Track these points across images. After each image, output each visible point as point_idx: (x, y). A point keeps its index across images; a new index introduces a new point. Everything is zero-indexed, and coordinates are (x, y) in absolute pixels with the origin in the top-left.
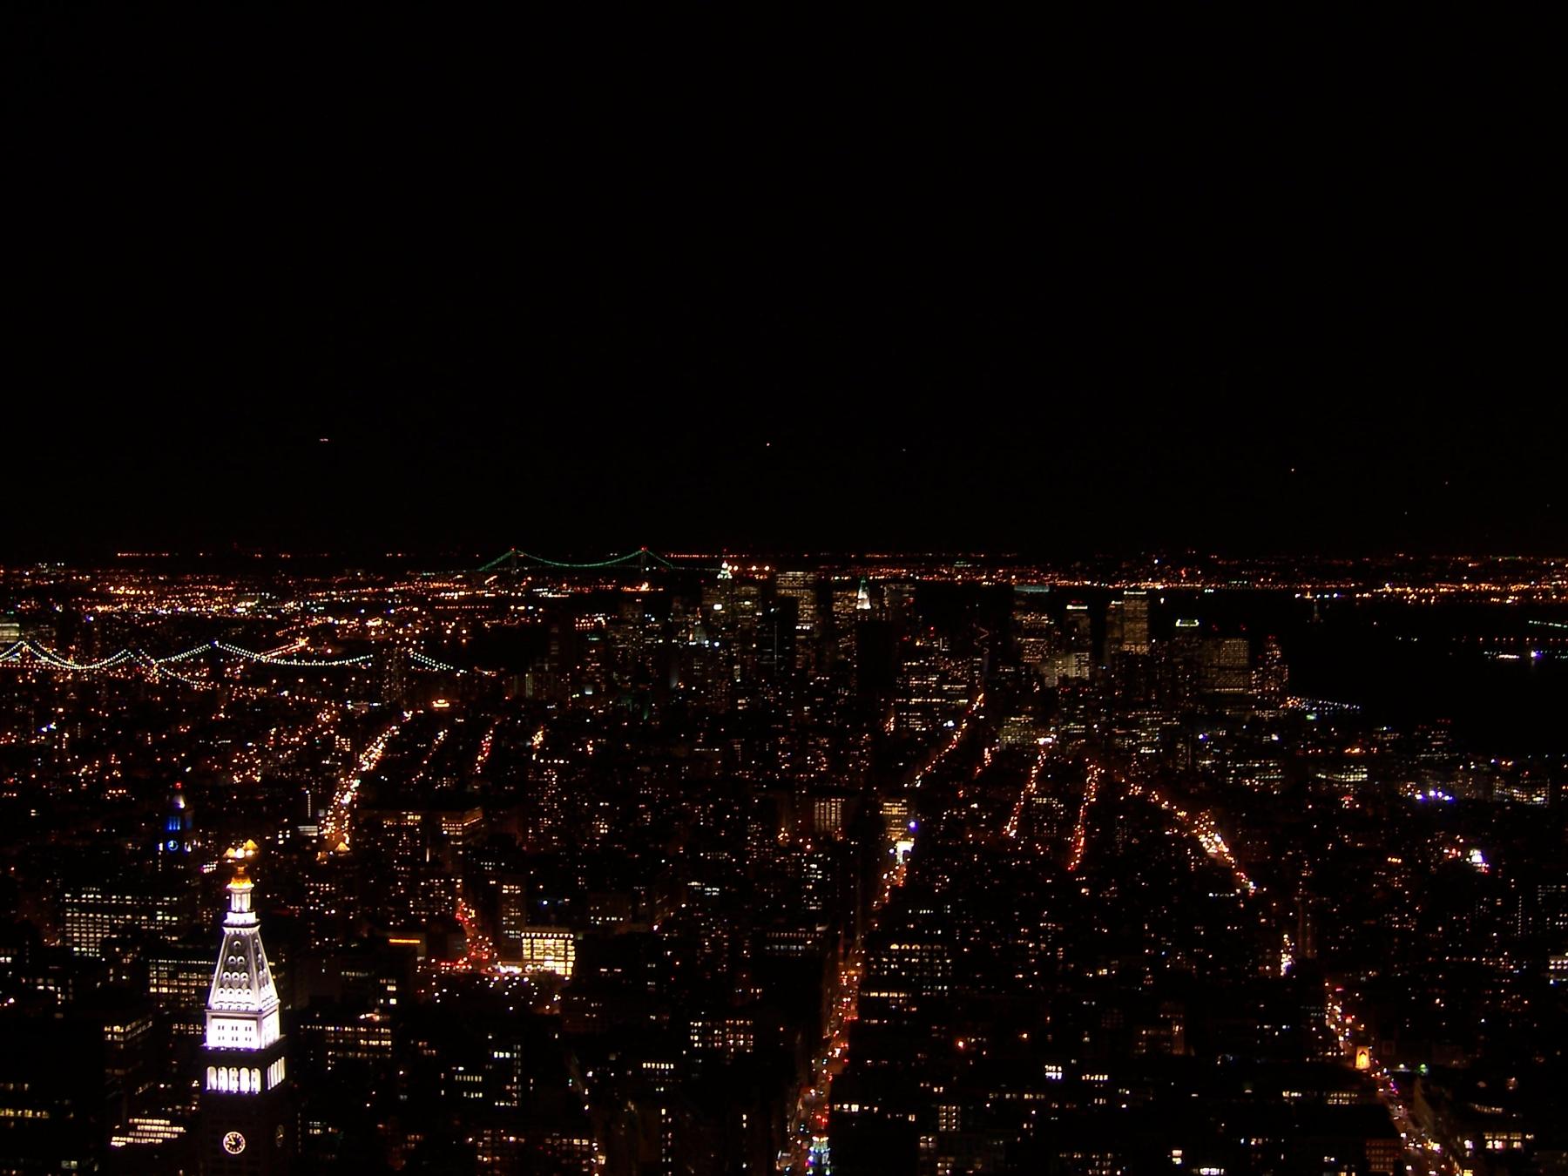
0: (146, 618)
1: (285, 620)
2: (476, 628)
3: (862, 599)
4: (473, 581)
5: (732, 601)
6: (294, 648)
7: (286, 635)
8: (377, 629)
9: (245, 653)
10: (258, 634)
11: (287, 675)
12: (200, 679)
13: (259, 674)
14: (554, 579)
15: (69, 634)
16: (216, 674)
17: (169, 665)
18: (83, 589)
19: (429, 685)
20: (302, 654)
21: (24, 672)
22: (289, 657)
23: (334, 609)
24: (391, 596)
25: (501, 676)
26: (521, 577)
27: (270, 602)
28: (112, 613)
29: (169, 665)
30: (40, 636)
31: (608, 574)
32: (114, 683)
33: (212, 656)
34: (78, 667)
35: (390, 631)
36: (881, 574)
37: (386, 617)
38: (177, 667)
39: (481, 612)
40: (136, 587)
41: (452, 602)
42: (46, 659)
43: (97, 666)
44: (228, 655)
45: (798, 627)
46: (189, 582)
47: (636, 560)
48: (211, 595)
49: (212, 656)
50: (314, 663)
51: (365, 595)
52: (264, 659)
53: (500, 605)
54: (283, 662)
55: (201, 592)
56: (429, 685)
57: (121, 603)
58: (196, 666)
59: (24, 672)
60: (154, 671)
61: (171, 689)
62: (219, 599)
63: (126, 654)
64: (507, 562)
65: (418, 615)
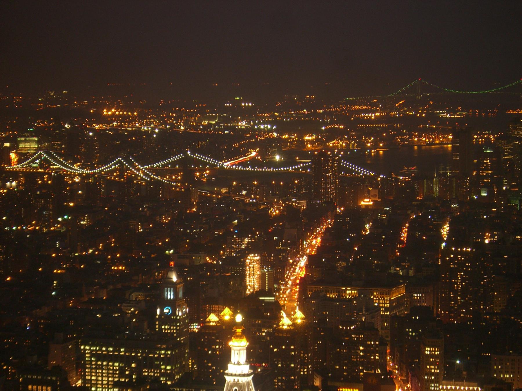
4: (388, 106)
6: (247, 158)
7: (241, 146)
8: (312, 142)
9: (211, 161)
16: (188, 176)
17: (152, 170)
20: (254, 162)
22: (243, 164)
28: (106, 129)
29: (152, 170)
30: (51, 147)
32: (111, 184)
33: (185, 163)
37: (318, 132)
38: (157, 172)
40: (123, 109)
41: (369, 121)
42: (58, 166)
44: (197, 162)
49: (185, 163)
50: (265, 169)
52: (227, 164)
57: (113, 122)
59: (42, 175)
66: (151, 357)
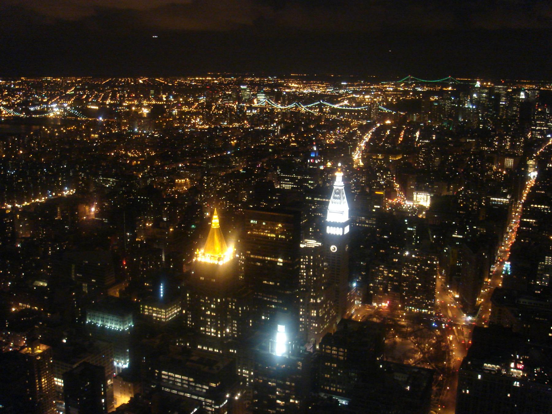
1: (341, 95)
2: (398, 100)
3: (522, 95)
5: (479, 94)
7: (341, 99)
8: (368, 99)
10: (333, 99)
11: (342, 112)
12: (316, 112)
13: (334, 111)
14: (422, 85)
15: (278, 97)
16: (321, 111)
17: (307, 108)
18: (281, 85)
19: (385, 116)
20: (346, 106)
21: (266, 108)
22: (342, 106)
23: (355, 92)
25: (406, 114)
26: (412, 84)
27: (337, 90)
28: (290, 92)
29: (307, 108)
30: (270, 98)
31: (438, 84)
32: (292, 112)
34: (281, 107)
35: (372, 99)
36: (526, 87)
37: (371, 95)
38: (311, 108)
39: (399, 94)
43: (287, 107)
44: (324, 105)
45: (501, 103)
46: (312, 83)
47: (448, 80)
48: (319, 87)
49: (320, 106)
50: (350, 108)
51: (365, 88)
53: (406, 93)
54: (341, 108)
55: (316, 86)
56: (385, 116)
58: (316, 108)
59: (266, 108)
60: (303, 109)
61: (309, 115)
62: (321, 88)
63: (295, 104)
64: (407, 80)
65: (380, 95)
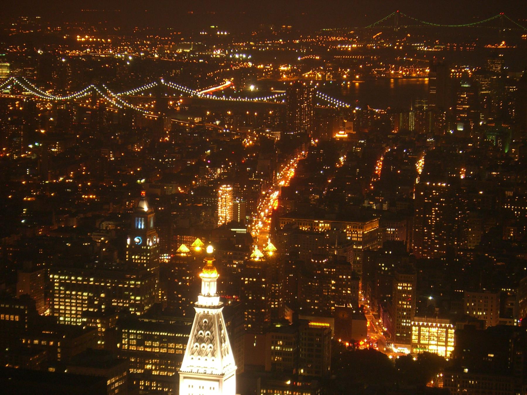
0: (105, 61)
1: (214, 63)
4: (364, 38)
6: (221, 87)
7: (215, 75)
8: (287, 73)
9: (185, 89)
16: (161, 106)
17: (125, 98)
20: (228, 91)
22: (218, 93)
24: (297, 46)
28: (79, 56)
29: (125, 98)
30: (24, 73)
33: (159, 91)
37: (293, 62)
38: (130, 100)
40: (96, 36)
41: (346, 52)
42: (31, 92)
44: (171, 91)
49: (159, 91)
50: (239, 99)
52: (199, 94)
57: (86, 48)
58: (146, 100)
59: (14, 100)
66: (68, 283)
